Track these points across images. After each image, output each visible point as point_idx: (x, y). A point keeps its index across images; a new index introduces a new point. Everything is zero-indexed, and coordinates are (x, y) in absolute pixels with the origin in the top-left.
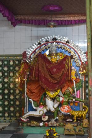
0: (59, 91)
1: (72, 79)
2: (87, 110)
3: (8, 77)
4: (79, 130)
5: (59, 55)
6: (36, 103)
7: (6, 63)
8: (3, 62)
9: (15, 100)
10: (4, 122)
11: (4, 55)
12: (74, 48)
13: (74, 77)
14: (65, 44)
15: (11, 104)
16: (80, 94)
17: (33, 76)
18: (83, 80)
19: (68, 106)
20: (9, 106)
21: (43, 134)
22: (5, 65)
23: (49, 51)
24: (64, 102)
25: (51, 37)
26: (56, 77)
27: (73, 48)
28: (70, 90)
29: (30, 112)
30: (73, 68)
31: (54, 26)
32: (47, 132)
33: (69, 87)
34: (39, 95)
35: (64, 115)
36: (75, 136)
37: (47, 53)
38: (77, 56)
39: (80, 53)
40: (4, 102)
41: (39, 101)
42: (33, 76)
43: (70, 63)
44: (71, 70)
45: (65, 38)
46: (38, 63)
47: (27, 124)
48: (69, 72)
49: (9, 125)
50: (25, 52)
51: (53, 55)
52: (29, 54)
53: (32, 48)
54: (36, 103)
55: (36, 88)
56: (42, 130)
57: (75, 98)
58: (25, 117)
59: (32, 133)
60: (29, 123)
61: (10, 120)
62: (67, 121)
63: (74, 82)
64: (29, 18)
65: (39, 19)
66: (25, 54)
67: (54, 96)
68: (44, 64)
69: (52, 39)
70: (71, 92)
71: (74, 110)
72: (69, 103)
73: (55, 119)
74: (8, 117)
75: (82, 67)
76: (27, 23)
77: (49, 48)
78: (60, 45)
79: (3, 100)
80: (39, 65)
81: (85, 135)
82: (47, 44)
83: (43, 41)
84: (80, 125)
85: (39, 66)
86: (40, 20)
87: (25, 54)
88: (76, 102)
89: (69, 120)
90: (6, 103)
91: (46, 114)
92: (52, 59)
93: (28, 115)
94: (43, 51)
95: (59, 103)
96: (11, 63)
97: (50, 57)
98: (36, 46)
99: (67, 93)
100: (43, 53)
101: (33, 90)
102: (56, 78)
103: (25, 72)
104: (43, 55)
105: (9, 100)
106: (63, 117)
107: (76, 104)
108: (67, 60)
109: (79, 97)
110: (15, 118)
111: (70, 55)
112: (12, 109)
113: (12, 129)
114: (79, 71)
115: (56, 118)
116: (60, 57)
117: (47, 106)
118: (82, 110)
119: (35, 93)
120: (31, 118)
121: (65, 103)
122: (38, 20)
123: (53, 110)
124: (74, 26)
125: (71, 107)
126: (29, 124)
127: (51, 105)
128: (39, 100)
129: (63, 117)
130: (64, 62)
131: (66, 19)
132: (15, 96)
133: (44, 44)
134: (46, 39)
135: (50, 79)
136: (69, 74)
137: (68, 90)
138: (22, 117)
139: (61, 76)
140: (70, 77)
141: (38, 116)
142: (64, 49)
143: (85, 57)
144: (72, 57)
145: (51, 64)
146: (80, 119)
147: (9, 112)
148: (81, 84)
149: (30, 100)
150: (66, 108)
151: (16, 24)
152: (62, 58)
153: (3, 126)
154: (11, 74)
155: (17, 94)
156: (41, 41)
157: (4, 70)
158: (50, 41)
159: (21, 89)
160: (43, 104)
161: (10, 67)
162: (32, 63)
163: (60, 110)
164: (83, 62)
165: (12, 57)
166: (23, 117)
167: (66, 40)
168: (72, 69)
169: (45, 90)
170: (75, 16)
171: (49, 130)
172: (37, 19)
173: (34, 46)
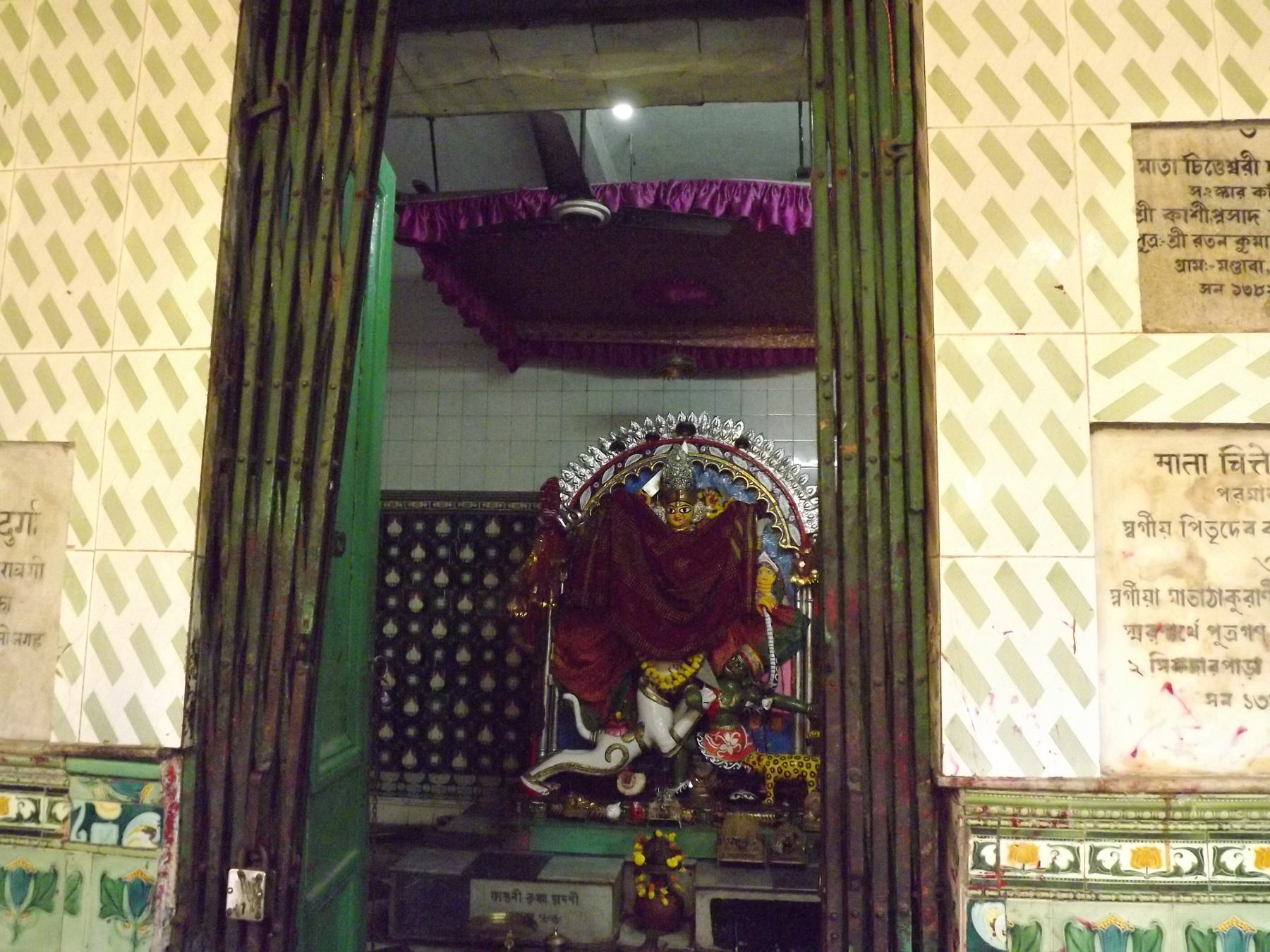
0: (697, 661)
3: (476, 589)
4: (785, 846)
5: (703, 500)
7: (468, 527)
9: (500, 696)
12: (771, 470)
13: (767, 599)
14: (734, 451)
17: (586, 587)
20: (474, 722)
21: (622, 856)
22: (466, 539)
24: (723, 710)
25: (671, 417)
30: (764, 557)
31: (687, 373)
32: (638, 846)
35: (718, 771)
37: (651, 488)
38: (785, 505)
41: (608, 705)
43: (750, 538)
44: (757, 566)
45: (731, 422)
47: (548, 808)
48: (745, 579)
49: (470, 812)
51: (678, 500)
52: (570, 489)
53: (586, 466)
56: (616, 838)
57: (770, 693)
58: (539, 775)
59: (568, 850)
62: (733, 798)
63: (769, 620)
66: (552, 488)
67: (677, 683)
69: (674, 427)
70: (755, 667)
71: (766, 750)
72: (740, 716)
73: (676, 790)
74: (466, 771)
75: (804, 557)
77: (660, 466)
78: (707, 452)
83: (634, 436)
84: (790, 817)
88: (776, 715)
90: (461, 709)
91: (635, 765)
93: (556, 767)
94: (633, 478)
96: (493, 528)
100: (631, 486)
106: (715, 782)
107: (778, 724)
108: (739, 524)
111: (750, 499)
112: (486, 736)
113: (481, 826)
114: (792, 574)
115: (682, 785)
117: (642, 726)
118: (803, 751)
120: (569, 780)
121: (724, 716)
123: (667, 744)
124: (774, 375)
125: (752, 738)
126: (557, 807)
127: (660, 724)
129: (715, 782)
130: (727, 531)
134: (648, 427)
135: (660, 605)
136: (744, 585)
138: (528, 777)
139: (709, 593)
140: (749, 599)
141: (598, 770)
142: (725, 472)
144: (762, 504)
146: (791, 790)
147: (474, 751)
148: (799, 631)
149: (568, 696)
152: (715, 511)
153: (441, 813)
154: (490, 580)
158: (665, 436)
159: (530, 648)
160: (623, 720)
162: (582, 531)
165: (497, 505)
166: (533, 773)
168: (761, 565)
169: (637, 654)
171: (649, 838)
173: (592, 454)
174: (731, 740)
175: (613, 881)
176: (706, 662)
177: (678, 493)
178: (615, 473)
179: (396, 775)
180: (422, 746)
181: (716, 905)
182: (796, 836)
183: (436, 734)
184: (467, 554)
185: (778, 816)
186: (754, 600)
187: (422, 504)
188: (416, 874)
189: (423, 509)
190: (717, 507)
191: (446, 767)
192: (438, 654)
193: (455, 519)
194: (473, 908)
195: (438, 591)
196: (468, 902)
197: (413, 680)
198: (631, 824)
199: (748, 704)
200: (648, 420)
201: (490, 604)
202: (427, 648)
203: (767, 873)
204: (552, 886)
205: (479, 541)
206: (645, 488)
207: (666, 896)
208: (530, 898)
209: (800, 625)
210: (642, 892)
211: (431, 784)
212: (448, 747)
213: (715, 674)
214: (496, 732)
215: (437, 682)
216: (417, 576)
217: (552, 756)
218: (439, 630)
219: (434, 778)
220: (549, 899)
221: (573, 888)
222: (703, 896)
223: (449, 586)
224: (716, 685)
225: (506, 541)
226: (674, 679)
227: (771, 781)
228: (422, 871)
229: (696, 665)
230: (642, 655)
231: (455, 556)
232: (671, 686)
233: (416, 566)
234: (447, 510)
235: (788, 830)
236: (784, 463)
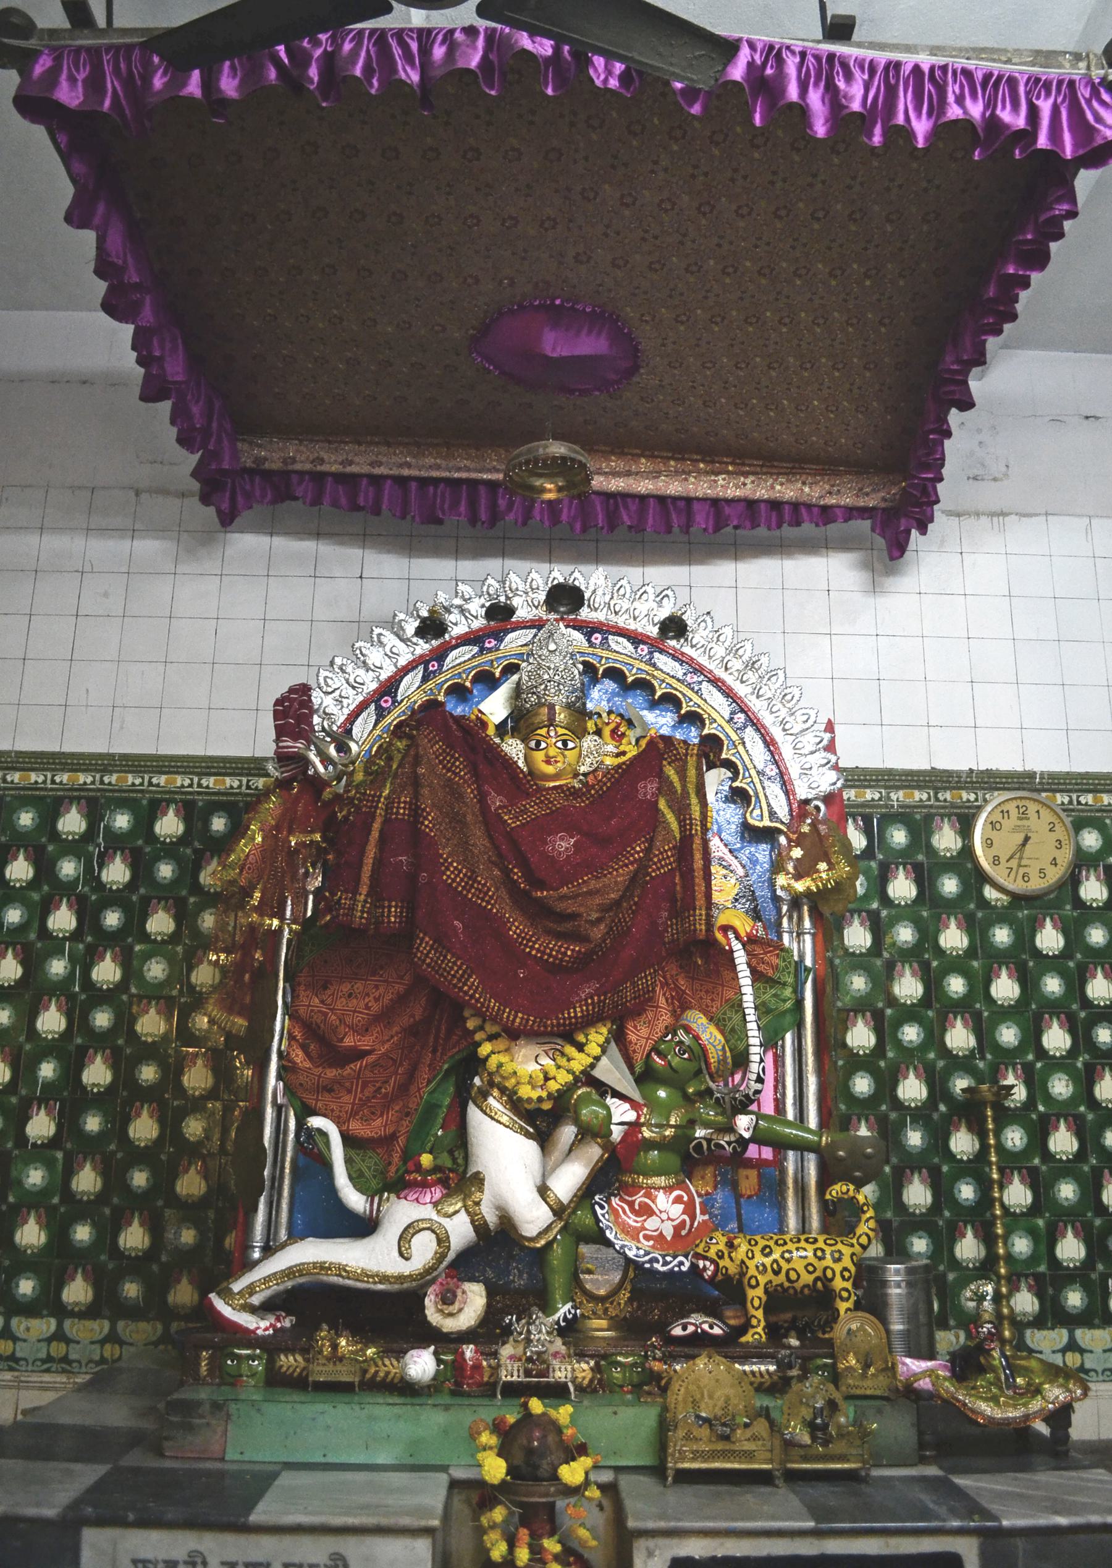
0: (596, 1037)
1: (719, 936)
2: (862, 1228)
3: (129, 943)
5: (598, 732)
6: (369, 1163)
7: (122, 821)
10: (49, 1359)
11: (113, 755)
12: (729, 680)
14: (656, 645)
15: (126, 1188)
16: (784, 1086)
17: (364, 890)
18: (808, 962)
19: (680, 1185)
21: (444, 1468)
22: (117, 843)
23: (518, 691)
24: (650, 1145)
26: (571, 907)
27: (716, 682)
28: (704, 1037)
29: (311, 1239)
32: (487, 1438)
33: (685, 1007)
34: (403, 1089)
36: (780, 1482)
37: (495, 707)
39: (783, 723)
40: (69, 1172)
41: (401, 1141)
42: (355, 892)
43: (694, 800)
46: (415, 782)
50: (304, 690)
51: (551, 722)
52: (332, 709)
54: (369, 1163)
55: (375, 1008)
58: (251, 1290)
59: (318, 1458)
60: (288, 1350)
61: (102, 1342)
62: (677, 1331)
63: (740, 957)
64: (351, 463)
65: (435, 474)
66: (294, 711)
67: (553, 1086)
68: (469, 792)
69: (542, 596)
70: (713, 1057)
71: (741, 1229)
76: (335, 504)
77: (511, 669)
79: (59, 1155)
80: (425, 791)
81: (876, 1473)
82: (498, 636)
83: (462, 611)
85: (426, 803)
86: (436, 481)
87: (294, 711)
90: (87, 1181)
91: (465, 1265)
92: (539, 756)
93: (289, 1273)
94: (458, 691)
95: (594, 1152)
96: (169, 825)
97: (523, 741)
98: (401, 647)
99: (676, 1062)
101: (354, 1029)
102: (574, 916)
103: (281, 861)
104: (459, 720)
105: (81, 998)
107: (749, 1181)
108: (671, 772)
109: (768, 1109)
112: (134, 1237)
113: (115, 1414)
115: (564, 1310)
116: (611, 748)
117: (478, 1180)
119: (371, 1059)
120: (317, 1303)
122: (424, 482)
123: (533, 1218)
124: (701, 561)
126: (289, 1362)
128: (406, 1126)
130: (650, 787)
131: (644, 486)
132: (170, 1123)
133: (472, 639)
135: (517, 927)
137: (682, 1035)
138: (226, 1295)
139: (617, 903)
141: (385, 1278)
143: (821, 757)
144: (712, 744)
145: (528, 795)
146: (802, 1310)
148: (788, 992)
149: (316, 1122)
150: (663, 1201)
151: (240, 499)
152: (618, 755)
153: (31, 1399)
155: (196, 1105)
156: (448, 610)
157: (99, 886)
160: (436, 1169)
161: (157, 859)
162: (359, 777)
163: (604, 1223)
164: (807, 802)
165: (179, 780)
166: (237, 1287)
167: (664, 613)
169: (471, 1024)
170: (717, 474)
171: (511, 1419)
172: (414, 473)
173: (381, 644)
174: (668, 1208)
175: (436, 1523)
176: (613, 1047)
177: (552, 707)
178: (425, 679)
182: (832, 1405)
184: (117, 873)
185: (783, 1366)
186: (709, 917)
187: (33, 777)
189: (35, 786)
190: (622, 748)
191: (49, 1303)
192: (47, 1070)
193: (95, 807)
195: (53, 945)
198: (456, 1393)
199: (700, 1133)
200: (490, 581)
201: (156, 970)
203: (785, 1496)
205: (141, 850)
206: (482, 707)
209: (790, 980)
210: (498, 1551)
213: (631, 1067)
214: (155, 1229)
217: (283, 1246)
222: (650, 1554)
223: (76, 935)
224: (636, 1095)
225: (198, 846)
226: (547, 1079)
227: (759, 1292)
229: (594, 1049)
230: (481, 1028)
231: (91, 877)
232: (544, 1094)
234: (83, 788)
235: (814, 1390)
236: (751, 665)
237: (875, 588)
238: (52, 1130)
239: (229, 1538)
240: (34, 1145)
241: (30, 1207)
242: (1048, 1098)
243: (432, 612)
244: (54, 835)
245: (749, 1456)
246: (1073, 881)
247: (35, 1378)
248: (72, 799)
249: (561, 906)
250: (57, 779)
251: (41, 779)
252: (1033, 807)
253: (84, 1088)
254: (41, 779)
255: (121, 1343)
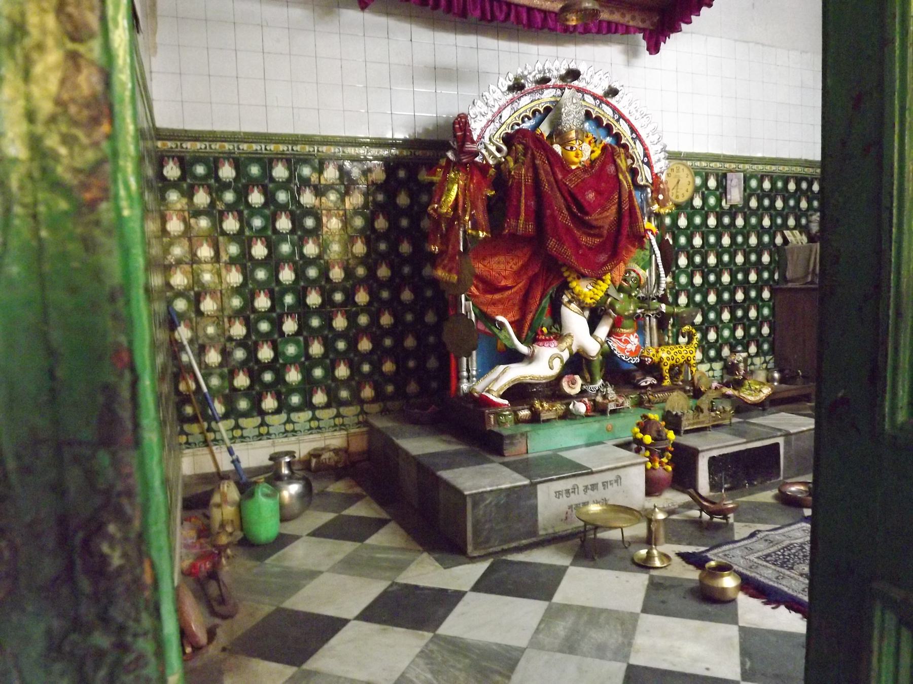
8: (295, 170)
10: (311, 428)
11: (297, 135)
15: (336, 350)
20: (330, 360)
26: (600, 223)
40: (307, 346)
42: (518, 219)
61: (334, 418)
74: (328, 406)
79: (301, 339)
89: (650, 380)
90: (316, 349)
101: (504, 277)
110: (359, 408)
112: (342, 371)
117: (569, 335)
119: (514, 290)
137: (633, 274)
141: (545, 378)
147: (331, 386)
179: (257, 420)
180: (280, 389)
181: (713, 461)
183: (293, 376)
187: (255, 147)
188: (491, 491)
189: (256, 152)
192: (289, 299)
194: (540, 509)
195: (282, 237)
196: (536, 507)
197: (264, 326)
202: (276, 292)
204: (603, 474)
207: (667, 464)
208: (586, 487)
211: (293, 423)
212: (308, 387)
215: (290, 326)
216: (257, 223)
218: (287, 275)
219: (294, 416)
220: (600, 485)
221: (616, 473)
223: (293, 231)
228: (495, 488)
233: (254, 211)
234: (283, 153)
237: (628, 64)
238: (296, 327)
239: (586, 477)
240: (288, 335)
241: (291, 364)
242: (679, 284)
243: (516, 79)
244: (272, 179)
245: (703, 422)
246: (692, 199)
247: (306, 437)
248: (278, 159)
249: (595, 223)
250: (268, 148)
251: (259, 148)
252: (682, 167)
253: (308, 306)
254: (259, 148)
255: (343, 417)
